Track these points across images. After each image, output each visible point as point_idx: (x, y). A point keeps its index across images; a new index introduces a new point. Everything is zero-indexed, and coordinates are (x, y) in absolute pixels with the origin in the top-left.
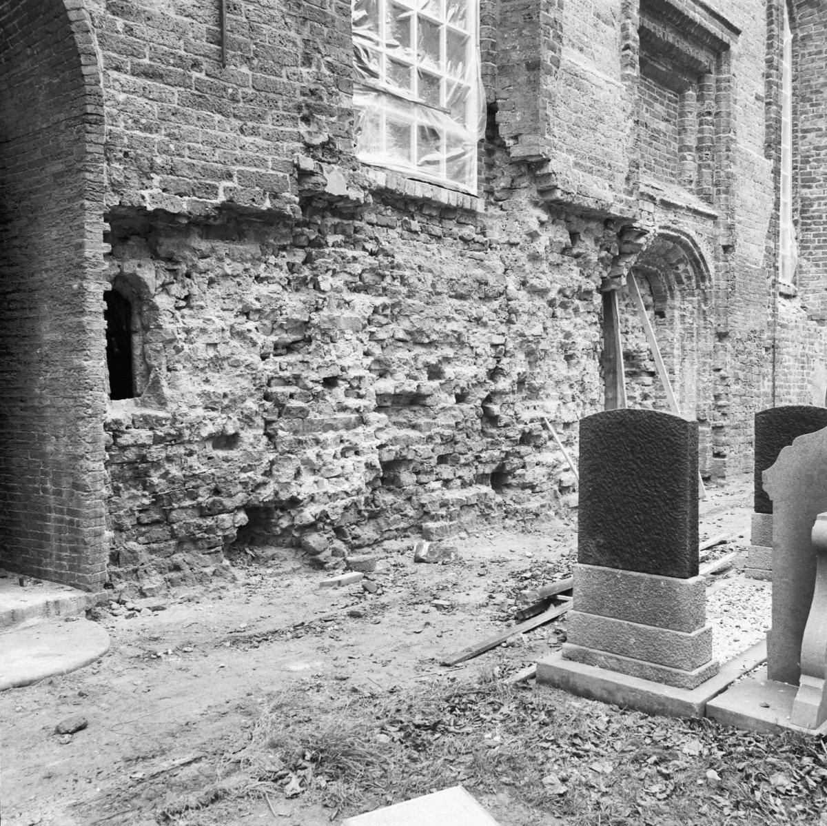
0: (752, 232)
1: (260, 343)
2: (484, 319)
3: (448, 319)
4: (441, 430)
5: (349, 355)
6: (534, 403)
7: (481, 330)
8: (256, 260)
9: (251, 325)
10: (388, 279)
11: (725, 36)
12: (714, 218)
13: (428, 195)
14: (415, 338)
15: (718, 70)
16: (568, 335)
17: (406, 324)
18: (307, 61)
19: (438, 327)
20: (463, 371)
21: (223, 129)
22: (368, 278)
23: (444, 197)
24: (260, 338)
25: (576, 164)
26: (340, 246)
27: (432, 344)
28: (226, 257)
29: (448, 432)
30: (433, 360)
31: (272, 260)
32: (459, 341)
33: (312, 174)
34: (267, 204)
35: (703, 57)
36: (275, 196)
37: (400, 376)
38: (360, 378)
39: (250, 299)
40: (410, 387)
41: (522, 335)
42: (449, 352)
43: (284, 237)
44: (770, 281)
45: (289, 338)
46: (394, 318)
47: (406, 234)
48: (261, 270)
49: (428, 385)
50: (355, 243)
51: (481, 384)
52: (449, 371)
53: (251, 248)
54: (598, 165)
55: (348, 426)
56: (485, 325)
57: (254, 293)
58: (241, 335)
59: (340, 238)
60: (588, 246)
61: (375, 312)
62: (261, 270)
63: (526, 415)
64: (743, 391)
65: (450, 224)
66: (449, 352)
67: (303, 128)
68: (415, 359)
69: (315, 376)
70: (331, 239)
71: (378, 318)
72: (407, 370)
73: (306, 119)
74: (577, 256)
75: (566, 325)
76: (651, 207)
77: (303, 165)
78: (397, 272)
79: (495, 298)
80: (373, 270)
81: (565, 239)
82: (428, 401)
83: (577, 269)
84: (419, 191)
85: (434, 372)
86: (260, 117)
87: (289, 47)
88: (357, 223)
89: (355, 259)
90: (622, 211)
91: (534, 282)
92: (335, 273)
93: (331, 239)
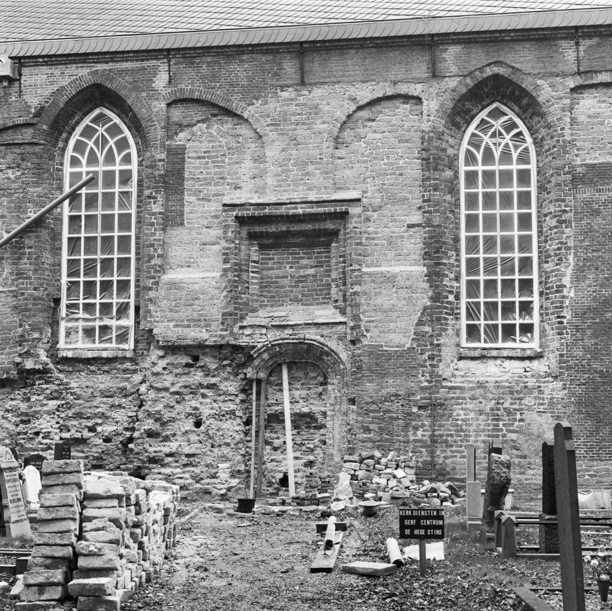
0: (392, 326)
1: (13, 421)
2: (124, 405)
3: (97, 407)
4: (92, 454)
5: (45, 424)
6: (165, 444)
7: (122, 410)
8: (10, 393)
9: (10, 415)
10: (64, 394)
12: (345, 323)
13: (95, 356)
14: (79, 416)
15: (345, 229)
16: (196, 409)
17: (73, 411)
18: (21, 326)
19: (89, 411)
20: (107, 429)
22: (55, 394)
23: (105, 354)
24: (14, 419)
25: (176, 326)
26: (42, 384)
27: (88, 418)
29: (95, 455)
30: (90, 424)
31: (17, 392)
32: (103, 416)
33: (20, 363)
34: (5, 376)
36: (8, 373)
37: (73, 431)
38: (49, 432)
39: (7, 406)
40: (79, 435)
41: (148, 411)
42: (99, 421)
43: (20, 384)
44: (425, 356)
45: (25, 418)
46: (69, 409)
47: (89, 373)
48: (12, 396)
49: (86, 434)
50: (50, 382)
51: (118, 434)
52: (99, 429)
53: (8, 390)
55: (43, 450)
56: (124, 408)
57: (9, 404)
58: (6, 418)
59: (41, 382)
61: (59, 406)
62: (12, 396)
63: (151, 449)
64: (379, 438)
65: (114, 365)
66: (99, 421)
67: (19, 348)
68: (80, 424)
69: (30, 432)
70: (37, 383)
71: (60, 409)
72: (76, 429)
73: (20, 345)
74: (202, 367)
75: (194, 403)
76: (264, 331)
77: (16, 361)
78: (69, 391)
79: (131, 395)
80: (56, 391)
82: (88, 441)
83: (202, 374)
84: (90, 355)
85: (92, 429)
86: (4, 349)
87: (14, 324)
88: (49, 375)
89: (47, 388)
90: (215, 341)
91: (159, 385)
92: (38, 395)
93: (37, 383)
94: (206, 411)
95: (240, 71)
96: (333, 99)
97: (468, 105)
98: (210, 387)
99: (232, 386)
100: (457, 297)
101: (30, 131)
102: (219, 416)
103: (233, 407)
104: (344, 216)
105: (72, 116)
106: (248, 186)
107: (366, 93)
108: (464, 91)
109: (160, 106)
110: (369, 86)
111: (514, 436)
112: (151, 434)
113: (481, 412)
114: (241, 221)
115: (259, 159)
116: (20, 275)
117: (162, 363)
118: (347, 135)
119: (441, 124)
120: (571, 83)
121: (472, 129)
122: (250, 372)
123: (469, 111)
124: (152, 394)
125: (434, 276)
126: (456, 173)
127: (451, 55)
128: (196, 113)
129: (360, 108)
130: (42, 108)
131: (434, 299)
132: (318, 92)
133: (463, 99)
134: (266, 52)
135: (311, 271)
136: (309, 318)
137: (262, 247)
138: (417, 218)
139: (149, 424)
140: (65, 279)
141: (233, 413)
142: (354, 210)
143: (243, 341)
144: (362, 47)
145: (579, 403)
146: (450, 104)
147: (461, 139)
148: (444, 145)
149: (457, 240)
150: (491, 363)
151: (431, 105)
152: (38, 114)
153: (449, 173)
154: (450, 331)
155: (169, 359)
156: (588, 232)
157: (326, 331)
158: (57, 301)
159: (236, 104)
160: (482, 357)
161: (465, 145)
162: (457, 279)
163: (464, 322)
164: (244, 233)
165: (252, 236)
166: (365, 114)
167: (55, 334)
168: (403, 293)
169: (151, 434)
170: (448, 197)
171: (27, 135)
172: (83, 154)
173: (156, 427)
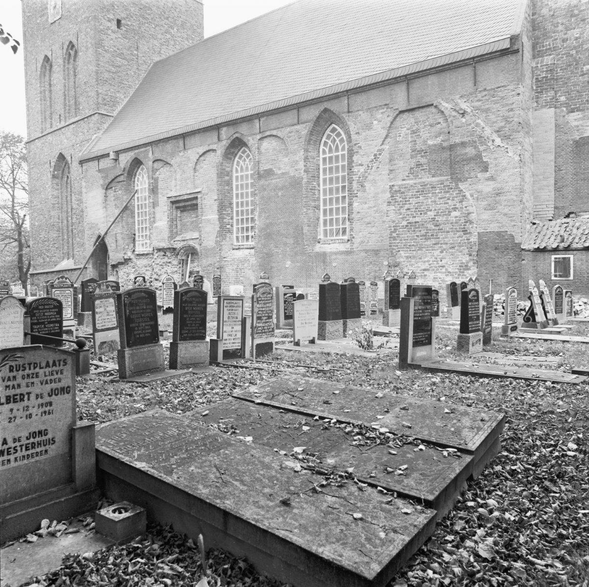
11: (195, 196)
21: (118, 254)
23: (145, 253)
28: (121, 267)
35: (194, 202)
54: (163, 240)
60: (168, 254)
81: (163, 253)
94: (169, 271)
95: (169, 147)
96: (193, 154)
97: (232, 150)
98: (170, 263)
99: (175, 262)
100: (232, 226)
101: (122, 176)
102: (173, 273)
103: (176, 269)
104: (196, 198)
105: (134, 169)
106: (174, 190)
107: (201, 150)
108: (227, 145)
109: (151, 163)
110: (201, 148)
111: (241, 278)
112: (156, 280)
113: (233, 270)
114: (173, 203)
115: (176, 180)
116: (123, 227)
117: (157, 255)
118: (198, 167)
119: (220, 159)
120: (258, 137)
121: (237, 159)
122: (179, 257)
123: (233, 152)
124: (155, 266)
125: (221, 219)
126: (231, 177)
127: (224, 131)
128: (160, 164)
129: (200, 156)
130: (125, 168)
131: (220, 228)
132: (189, 152)
133: (228, 148)
134: (175, 139)
135: (195, 219)
136: (190, 236)
137: (182, 211)
138: (216, 198)
139: (155, 276)
140: (137, 227)
141: (176, 271)
142: (199, 196)
143: (175, 246)
144: (199, 133)
145: (260, 265)
146: (224, 151)
147: (233, 164)
148: (224, 167)
149: (231, 204)
150: (241, 250)
151: (219, 152)
152: (124, 171)
153: (227, 178)
154: (228, 239)
155: (159, 253)
156: (262, 198)
157: (195, 241)
158: (135, 235)
159: (168, 160)
160: (239, 249)
161: (235, 166)
162: (232, 219)
163: (235, 235)
164: (174, 206)
165: (177, 208)
166: (202, 158)
167: (134, 246)
168: (212, 226)
169: (156, 280)
170: (227, 187)
171: (121, 178)
172: (326, 147)
173: (157, 277)
